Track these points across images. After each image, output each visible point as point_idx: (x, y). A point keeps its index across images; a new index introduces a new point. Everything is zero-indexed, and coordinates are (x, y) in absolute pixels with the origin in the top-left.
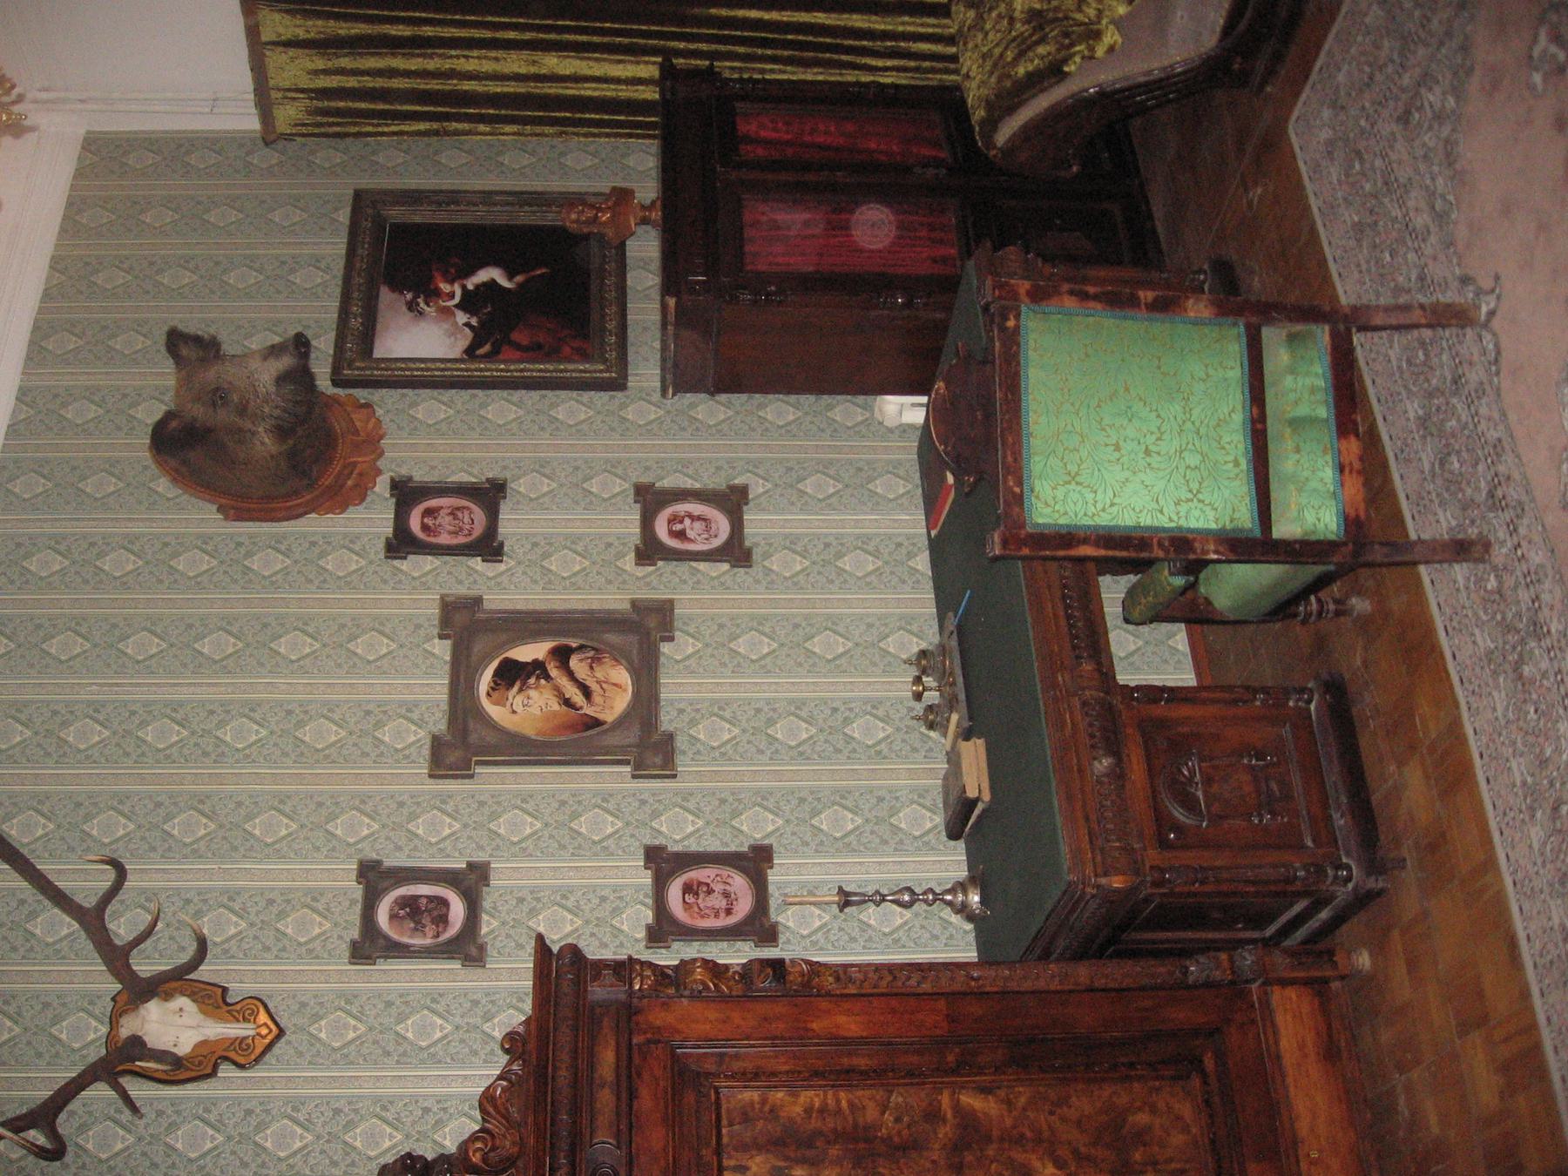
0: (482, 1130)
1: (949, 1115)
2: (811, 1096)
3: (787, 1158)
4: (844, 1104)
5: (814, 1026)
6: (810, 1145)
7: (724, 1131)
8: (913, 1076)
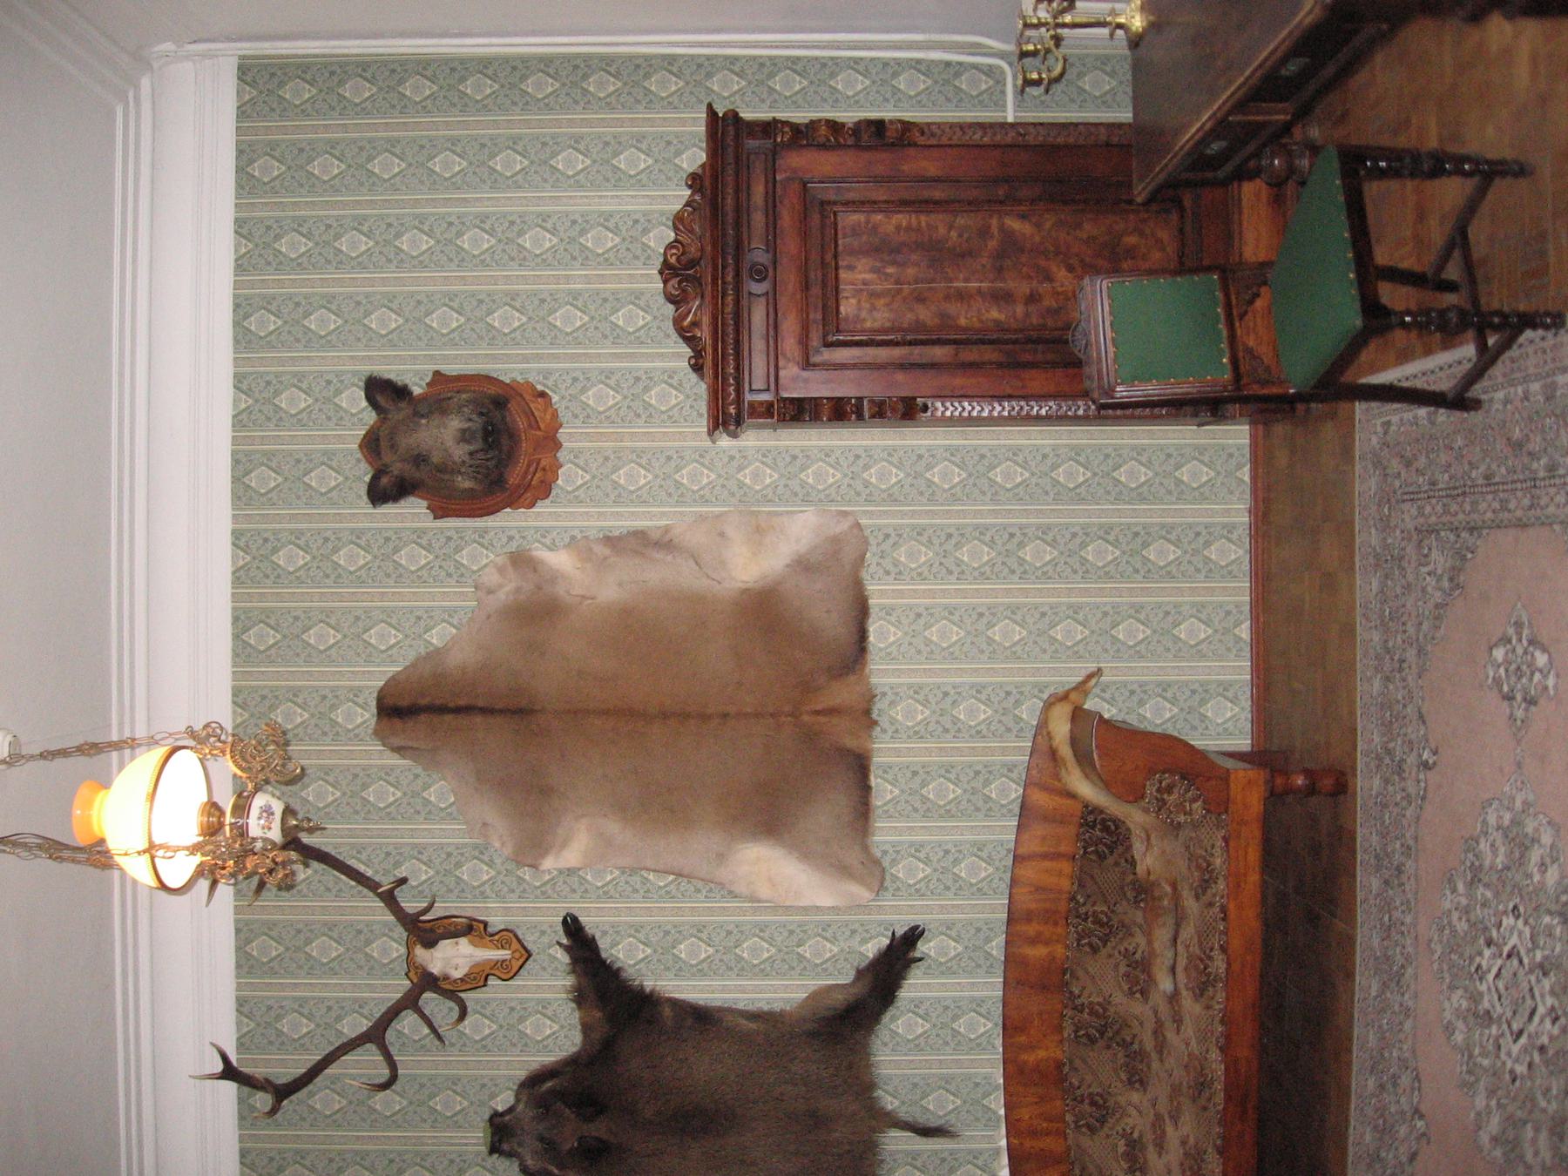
0: (676, 241)
1: (996, 233)
2: (902, 219)
3: (882, 261)
4: (923, 224)
5: (905, 168)
6: (899, 252)
7: (840, 242)
8: (973, 205)
